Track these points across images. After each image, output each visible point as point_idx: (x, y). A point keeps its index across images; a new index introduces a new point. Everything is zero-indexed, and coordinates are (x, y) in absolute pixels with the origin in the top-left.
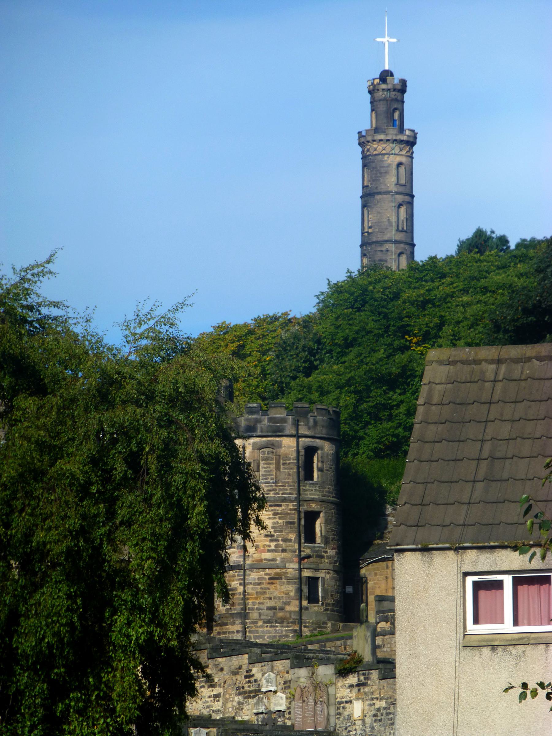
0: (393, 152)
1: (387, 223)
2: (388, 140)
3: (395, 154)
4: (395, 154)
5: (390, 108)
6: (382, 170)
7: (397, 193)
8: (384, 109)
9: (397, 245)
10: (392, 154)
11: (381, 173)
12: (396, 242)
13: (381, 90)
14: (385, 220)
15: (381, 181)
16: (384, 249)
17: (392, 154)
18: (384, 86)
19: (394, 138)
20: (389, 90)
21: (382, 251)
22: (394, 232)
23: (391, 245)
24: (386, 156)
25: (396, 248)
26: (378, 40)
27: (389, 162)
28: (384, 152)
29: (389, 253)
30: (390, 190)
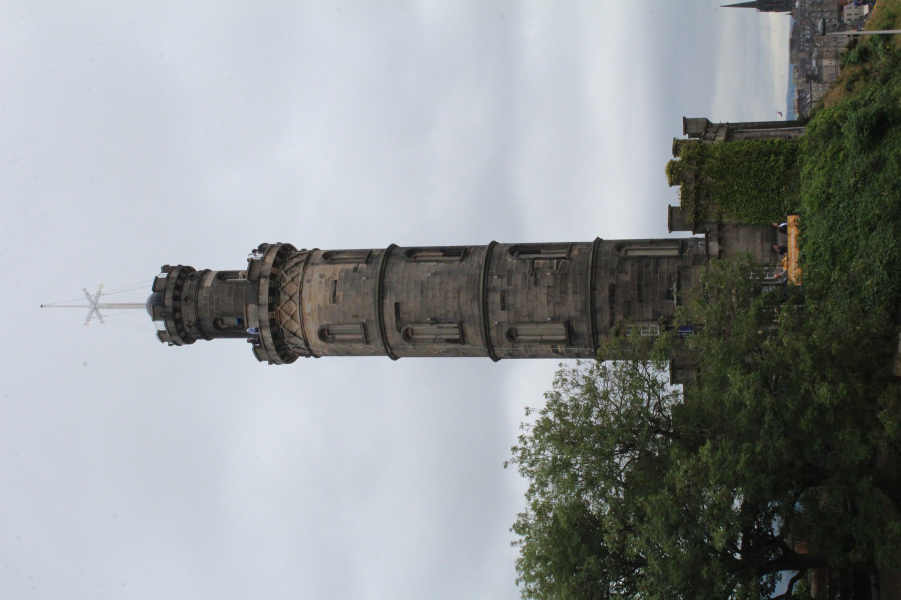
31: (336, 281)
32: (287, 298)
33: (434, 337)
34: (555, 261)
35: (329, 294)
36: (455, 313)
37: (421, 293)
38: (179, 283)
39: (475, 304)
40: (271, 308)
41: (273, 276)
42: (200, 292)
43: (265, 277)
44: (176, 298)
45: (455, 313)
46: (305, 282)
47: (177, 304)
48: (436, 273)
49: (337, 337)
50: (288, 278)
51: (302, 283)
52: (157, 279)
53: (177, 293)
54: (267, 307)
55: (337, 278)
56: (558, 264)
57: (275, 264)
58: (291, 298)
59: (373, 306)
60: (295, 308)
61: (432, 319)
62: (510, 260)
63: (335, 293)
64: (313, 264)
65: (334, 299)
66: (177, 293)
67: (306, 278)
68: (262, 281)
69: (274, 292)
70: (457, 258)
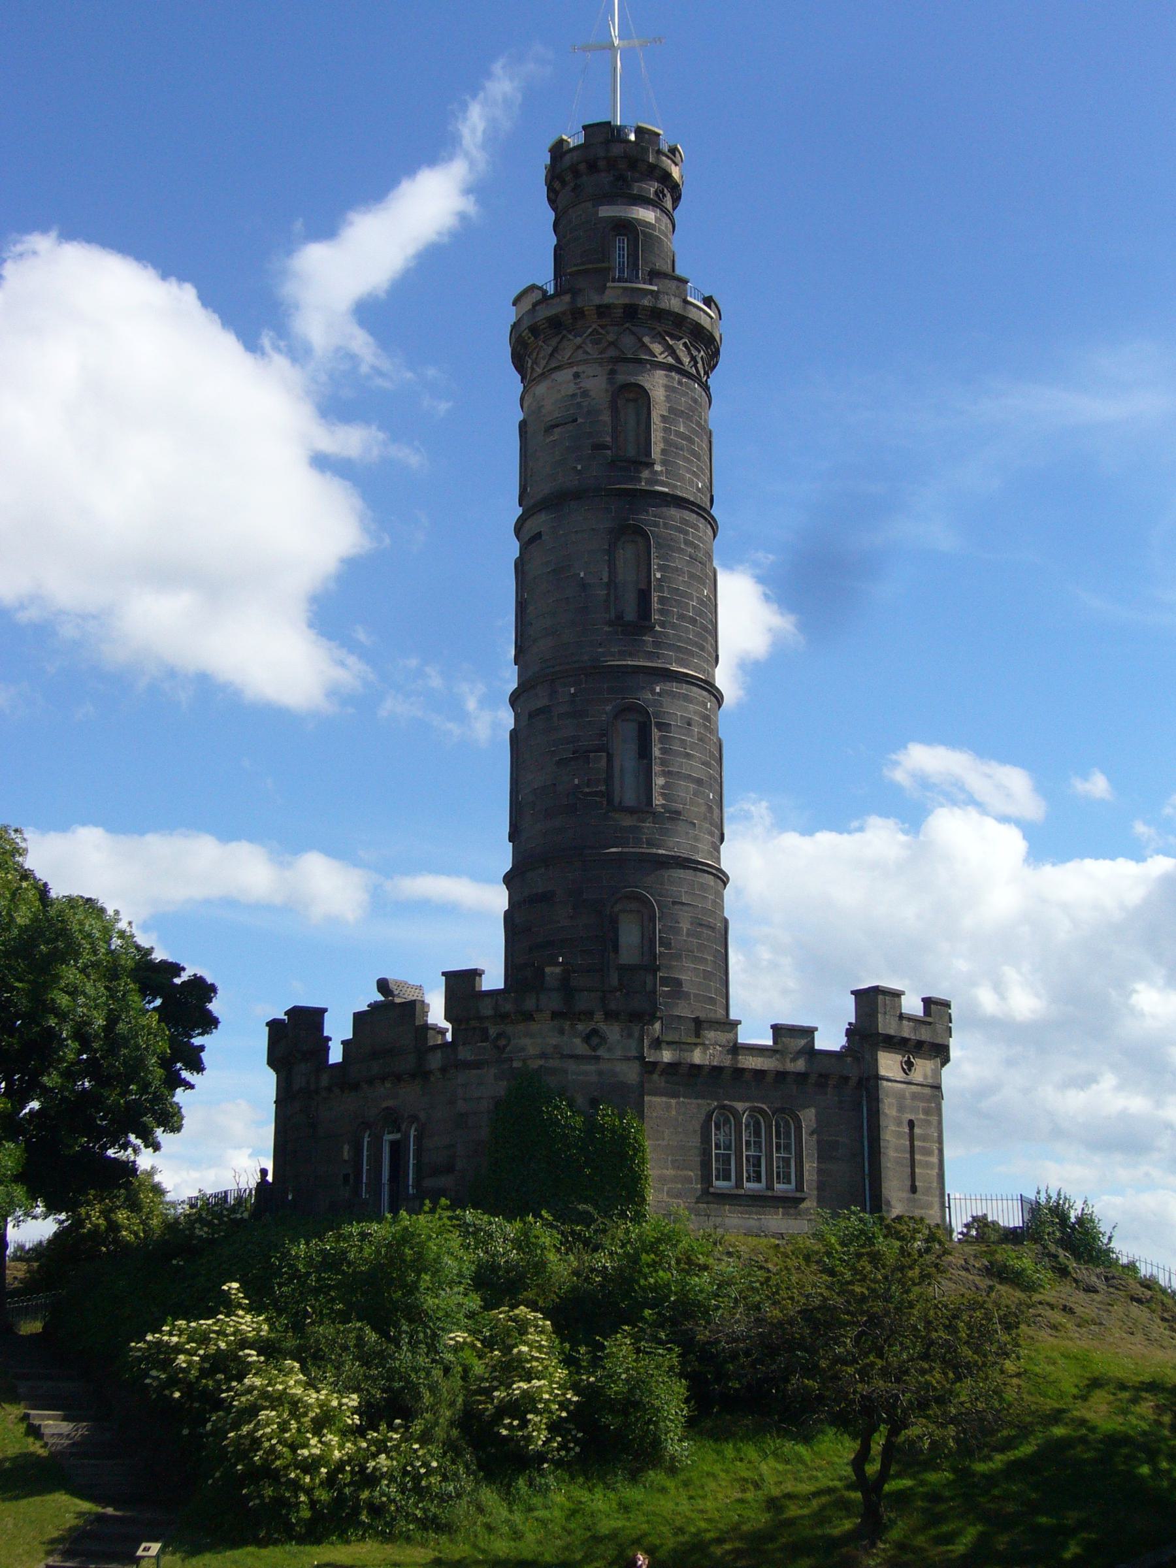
31: (576, 420)
34: (603, 788)
38: (602, 164)
41: (578, 314)
47: (569, 177)
48: (584, 586)
50: (579, 340)
53: (582, 167)
55: (580, 420)
56: (595, 794)
57: (603, 310)
60: (539, 370)
62: (609, 708)
63: (557, 426)
64: (612, 372)
67: (579, 369)
68: (567, 298)
70: (630, 615)
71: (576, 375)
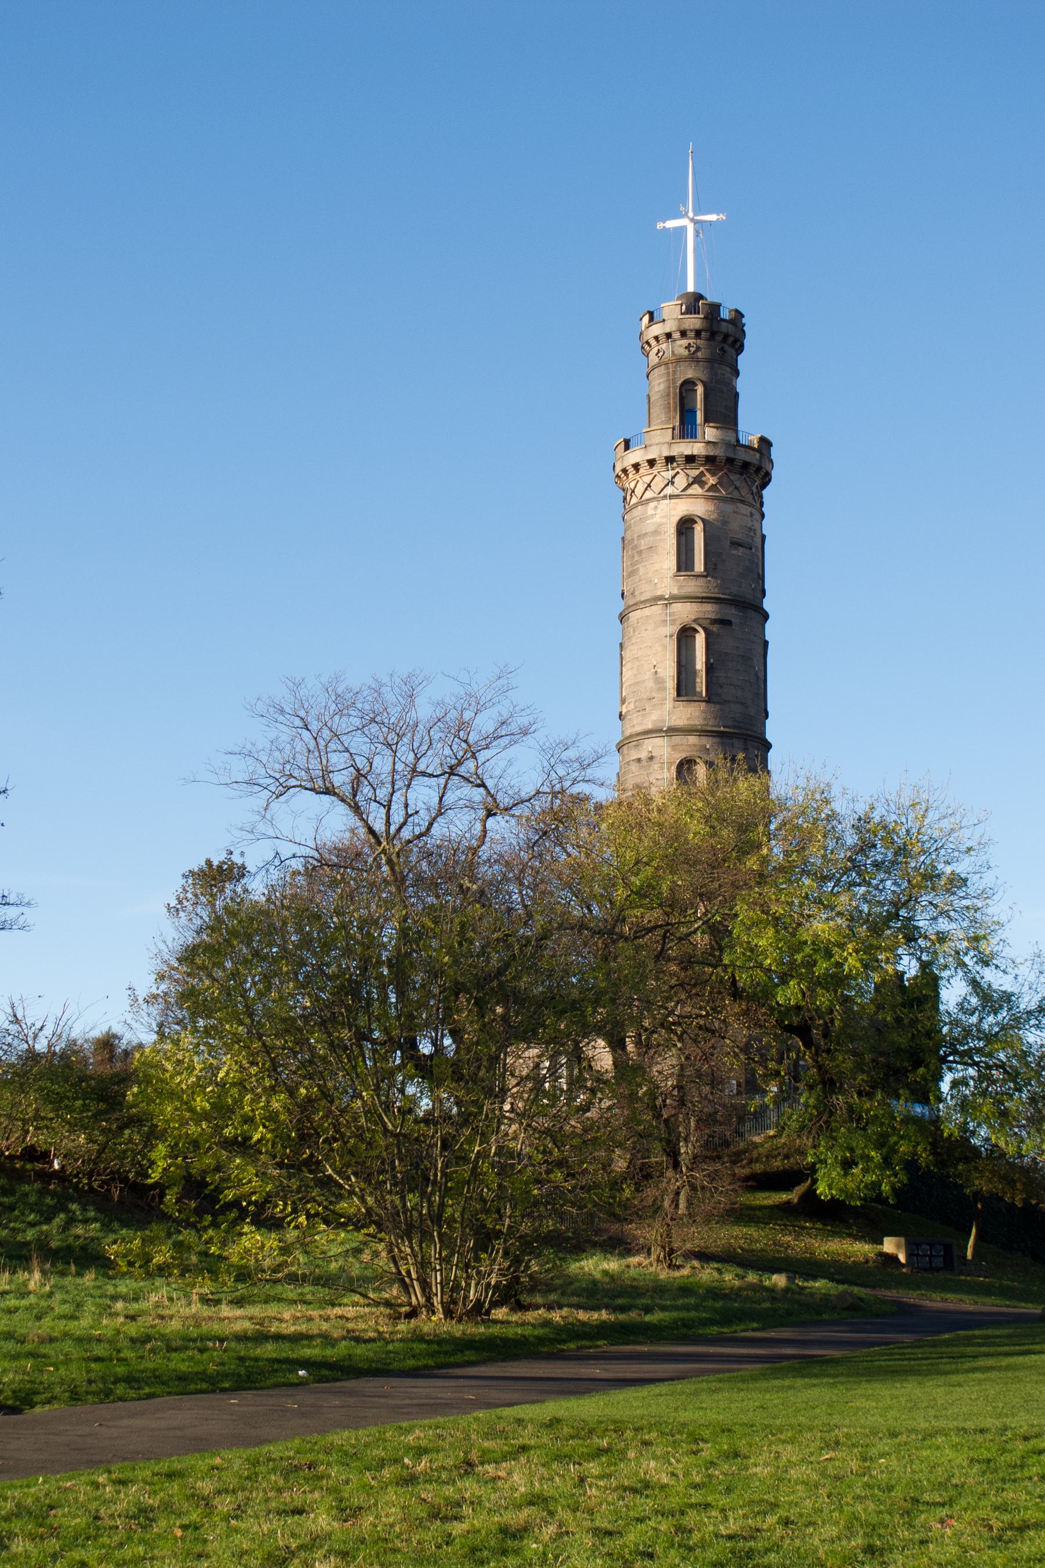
0: (669, 490)
1: (650, 684)
2: (652, 463)
3: (672, 497)
4: (672, 497)
5: (674, 380)
6: (644, 544)
7: (675, 598)
8: (662, 387)
9: (677, 739)
10: (665, 497)
11: (640, 552)
12: (672, 731)
13: (653, 342)
14: (648, 675)
15: (642, 571)
16: (643, 755)
17: (665, 497)
18: (657, 330)
19: (666, 453)
20: (669, 336)
21: (639, 760)
22: (669, 704)
23: (658, 741)
24: (652, 505)
25: (674, 747)
26: (671, 224)
27: (657, 519)
28: (649, 494)
29: (655, 766)
30: (659, 593)
31: (751, 549)
32: (738, 484)
33: (683, 663)
35: (740, 536)
36: (720, 695)
37: (743, 657)
39: (729, 723)
40: (730, 461)
41: (759, 469)
42: (728, 369)
43: (760, 460)
44: (726, 336)
45: (720, 695)
46: (750, 509)
47: (719, 338)
49: (683, 538)
51: (751, 505)
52: (743, 316)
53: (731, 339)
54: (732, 456)
58: (737, 488)
59: (728, 591)
61: (712, 664)
63: (740, 545)
65: (736, 544)
66: (731, 339)
69: (746, 465)
71: (752, 515)
